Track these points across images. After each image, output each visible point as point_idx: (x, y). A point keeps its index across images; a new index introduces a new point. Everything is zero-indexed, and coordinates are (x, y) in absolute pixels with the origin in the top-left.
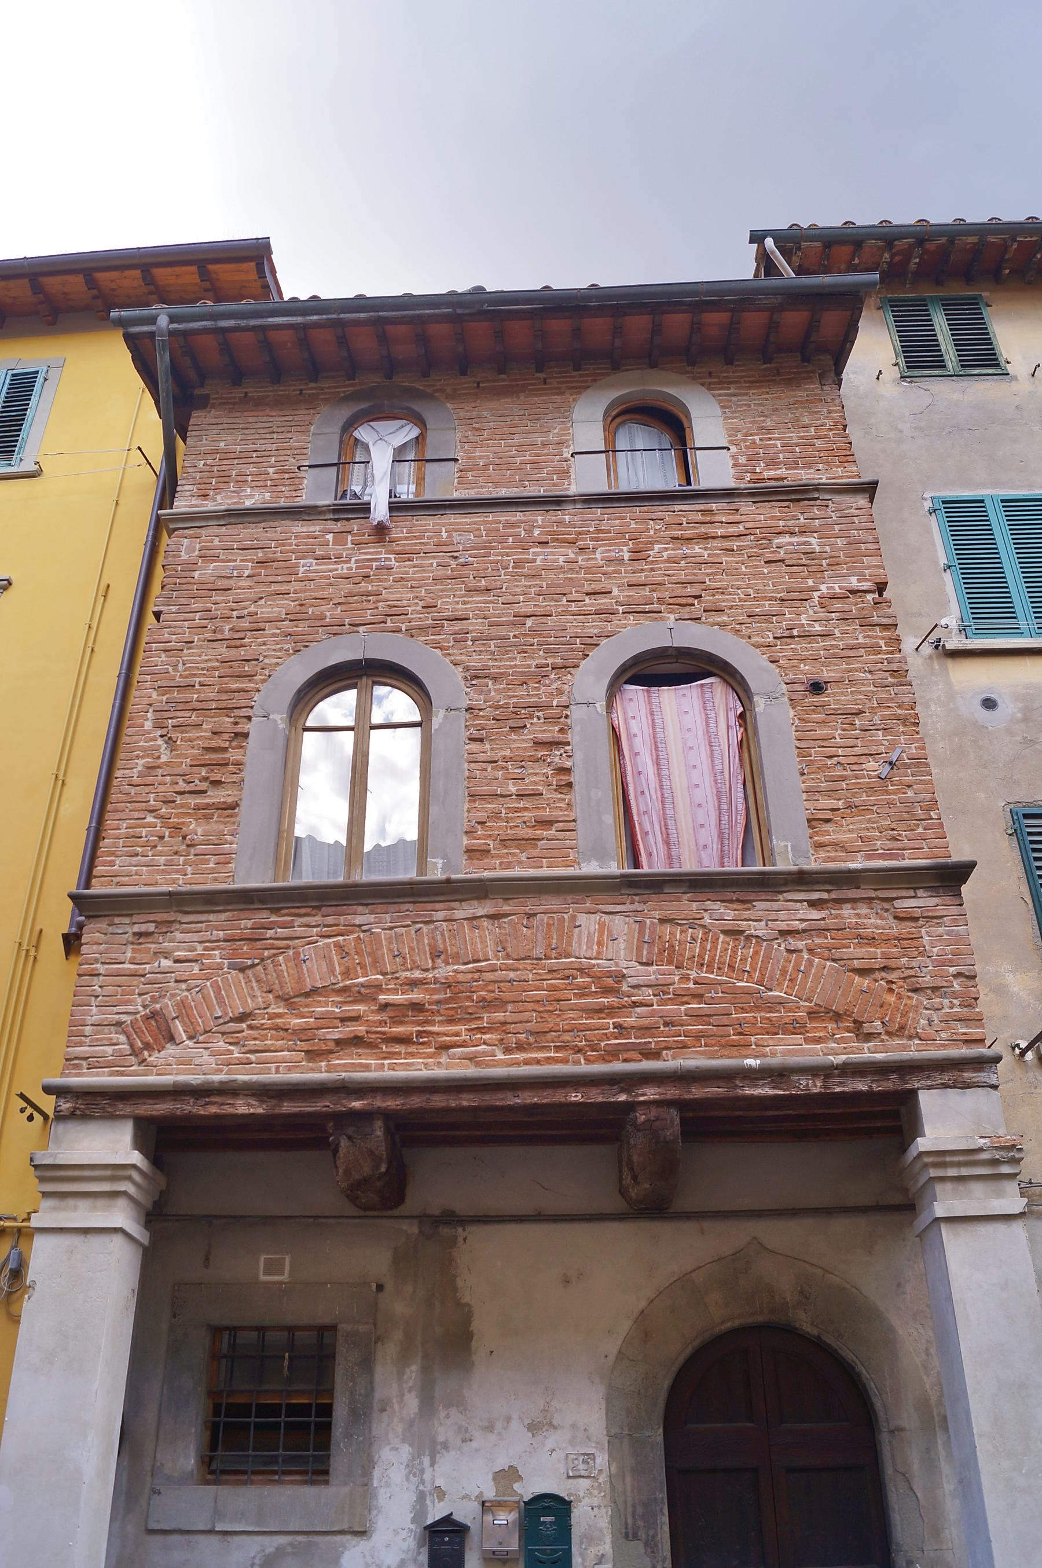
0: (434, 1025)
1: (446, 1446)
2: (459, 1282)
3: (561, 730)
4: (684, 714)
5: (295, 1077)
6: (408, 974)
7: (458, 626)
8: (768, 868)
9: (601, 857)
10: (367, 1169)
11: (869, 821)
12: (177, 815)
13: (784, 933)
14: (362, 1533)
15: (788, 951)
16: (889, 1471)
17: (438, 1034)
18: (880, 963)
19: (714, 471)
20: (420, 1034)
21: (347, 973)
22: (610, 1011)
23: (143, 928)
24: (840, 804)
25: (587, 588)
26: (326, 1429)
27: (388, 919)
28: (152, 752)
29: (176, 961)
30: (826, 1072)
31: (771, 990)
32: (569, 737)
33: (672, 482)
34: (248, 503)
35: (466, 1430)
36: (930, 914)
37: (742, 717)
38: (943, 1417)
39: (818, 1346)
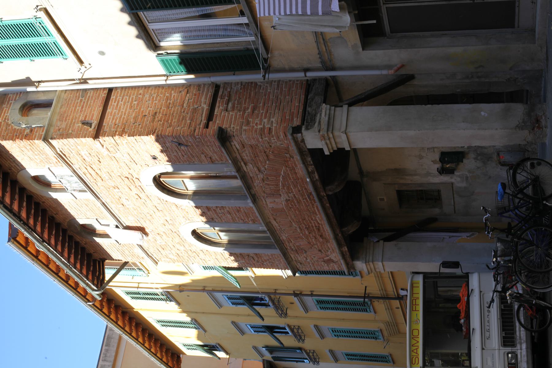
20: (316, 227)
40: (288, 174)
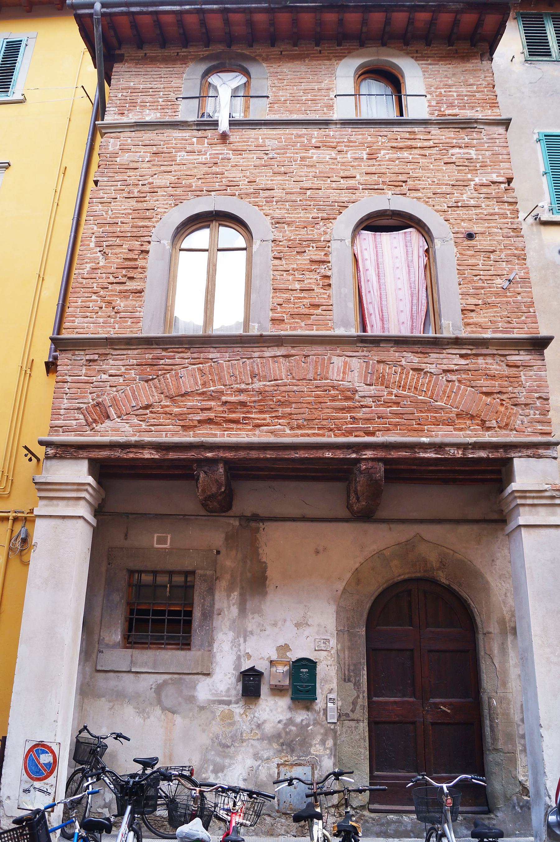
0: (252, 414)
1: (252, 633)
2: (260, 551)
3: (325, 254)
4: (395, 250)
5: (176, 439)
6: (238, 386)
8: (438, 335)
9: (346, 325)
10: (214, 490)
11: (496, 312)
12: (109, 296)
13: (445, 371)
14: (208, 675)
15: (447, 381)
16: (482, 653)
17: (254, 419)
18: (497, 389)
19: (416, 109)
20: (244, 418)
21: (204, 384)
22: (349, 409)
23: (92, 357)
24: (480, 302)
25: (342, 174)
26: (189, 623)
27: (228, 356)
28: (94, 260)
29: (110, 376)
30: (464, 446)
31: (437, 401)
32: (330, 258)
33: (393, 114)
34: (148, 119)
35: (263, 625)
36: (526, 364)
37: (427, 251)
38: (511, 629)
39: (448, 590)
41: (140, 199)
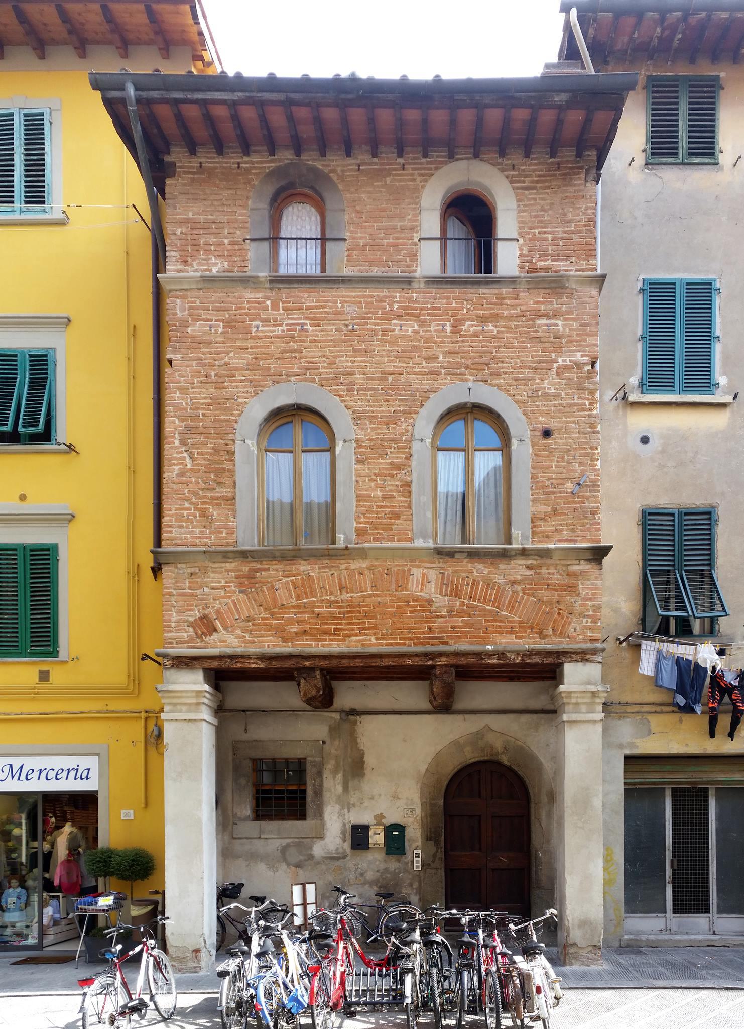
1: (354, 805)
5: (278, 650)
7: (349, 379)
10: (314, 693)
11: (563, 520)
12: (202, 503)
20: (335, 629)
23: (193, 570)
40: (501, 621)
41: (219, 386)
